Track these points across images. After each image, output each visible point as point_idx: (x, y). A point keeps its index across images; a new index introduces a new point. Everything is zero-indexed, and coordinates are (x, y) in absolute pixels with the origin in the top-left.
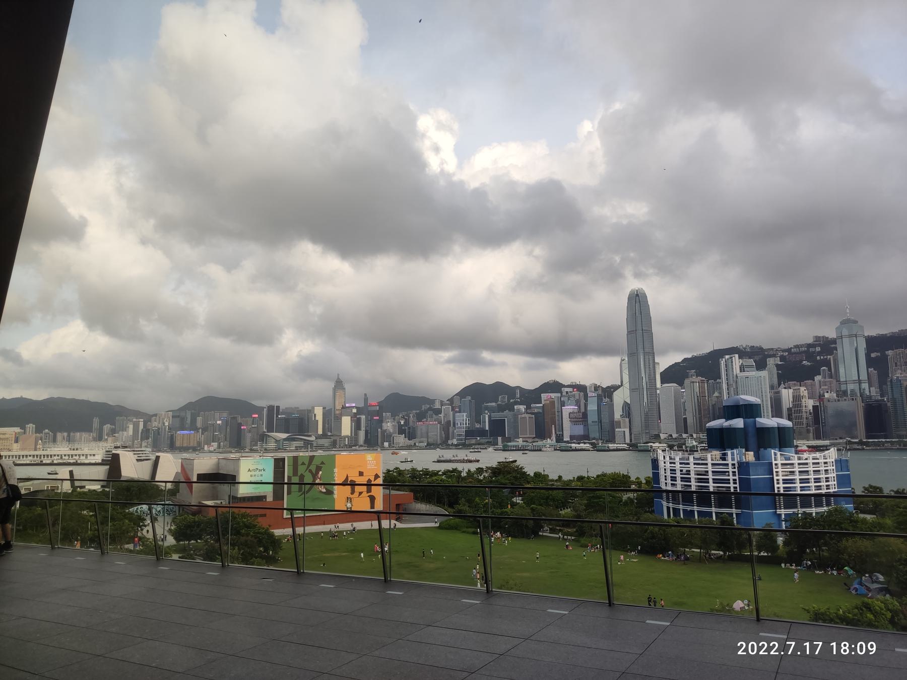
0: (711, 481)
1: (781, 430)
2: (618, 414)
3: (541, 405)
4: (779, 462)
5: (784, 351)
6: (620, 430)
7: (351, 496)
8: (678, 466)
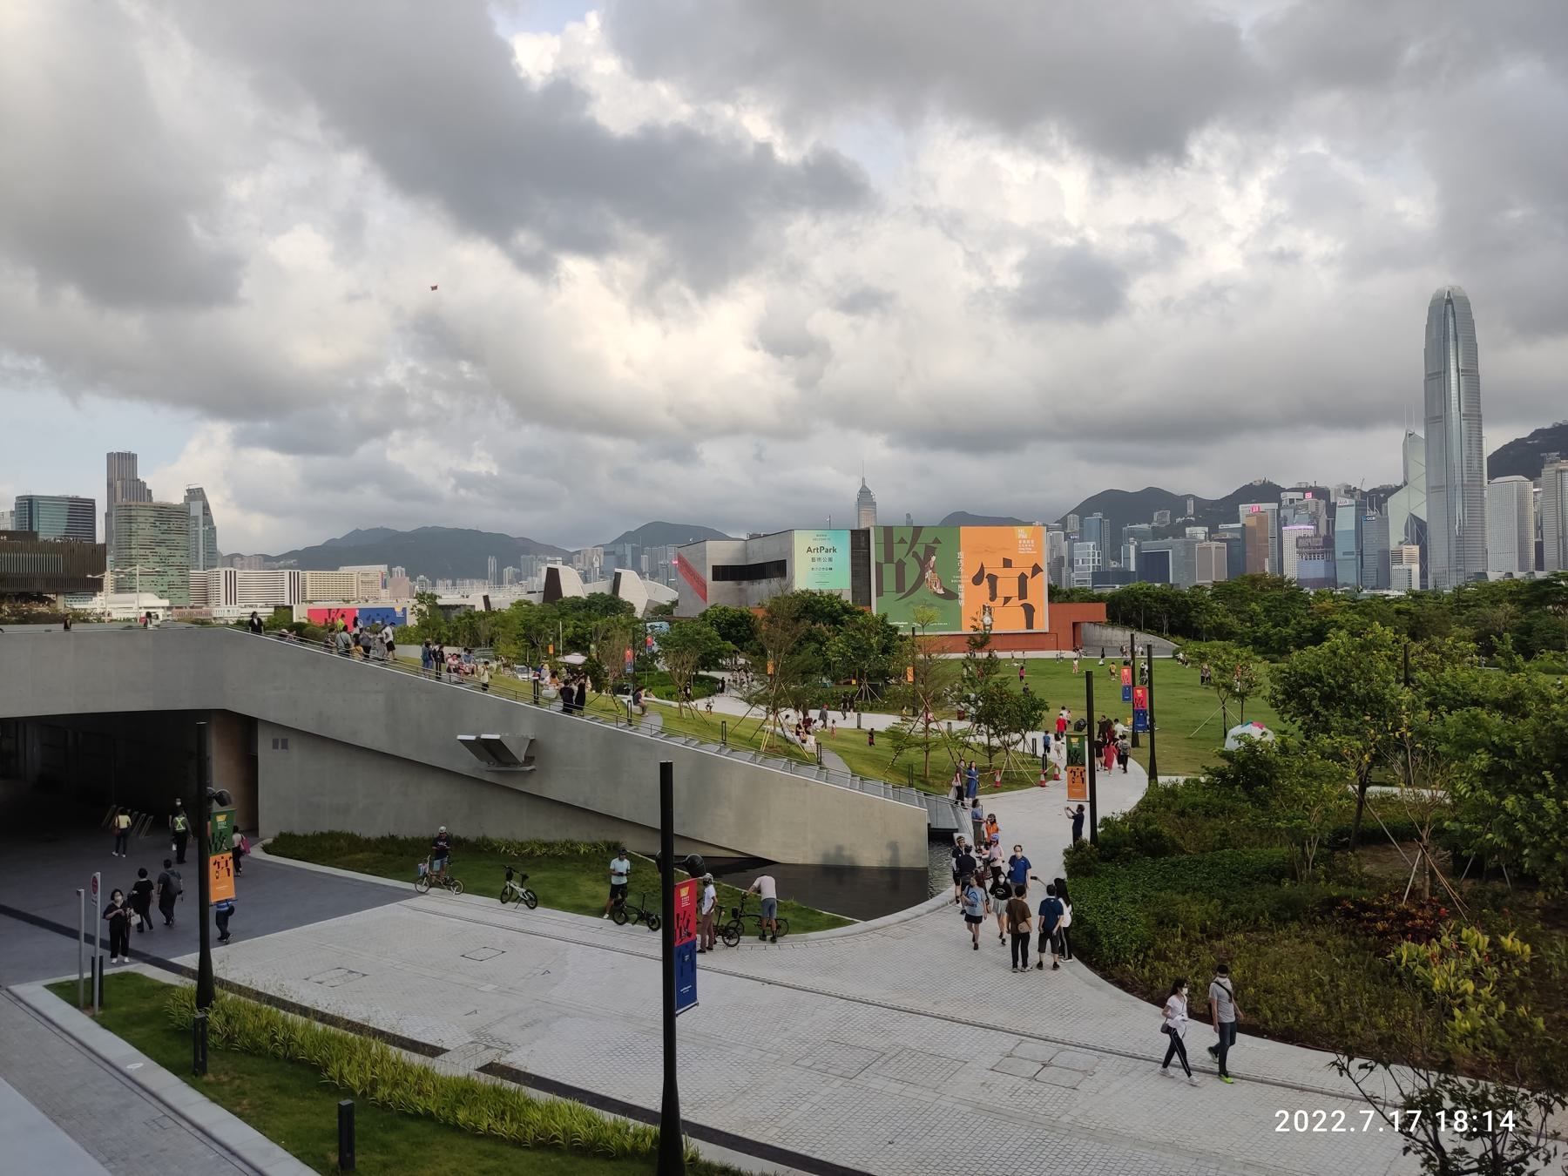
2: (1396, 535)
3: (1239, 525)
6: (1401, 567)
7: (991, 604)
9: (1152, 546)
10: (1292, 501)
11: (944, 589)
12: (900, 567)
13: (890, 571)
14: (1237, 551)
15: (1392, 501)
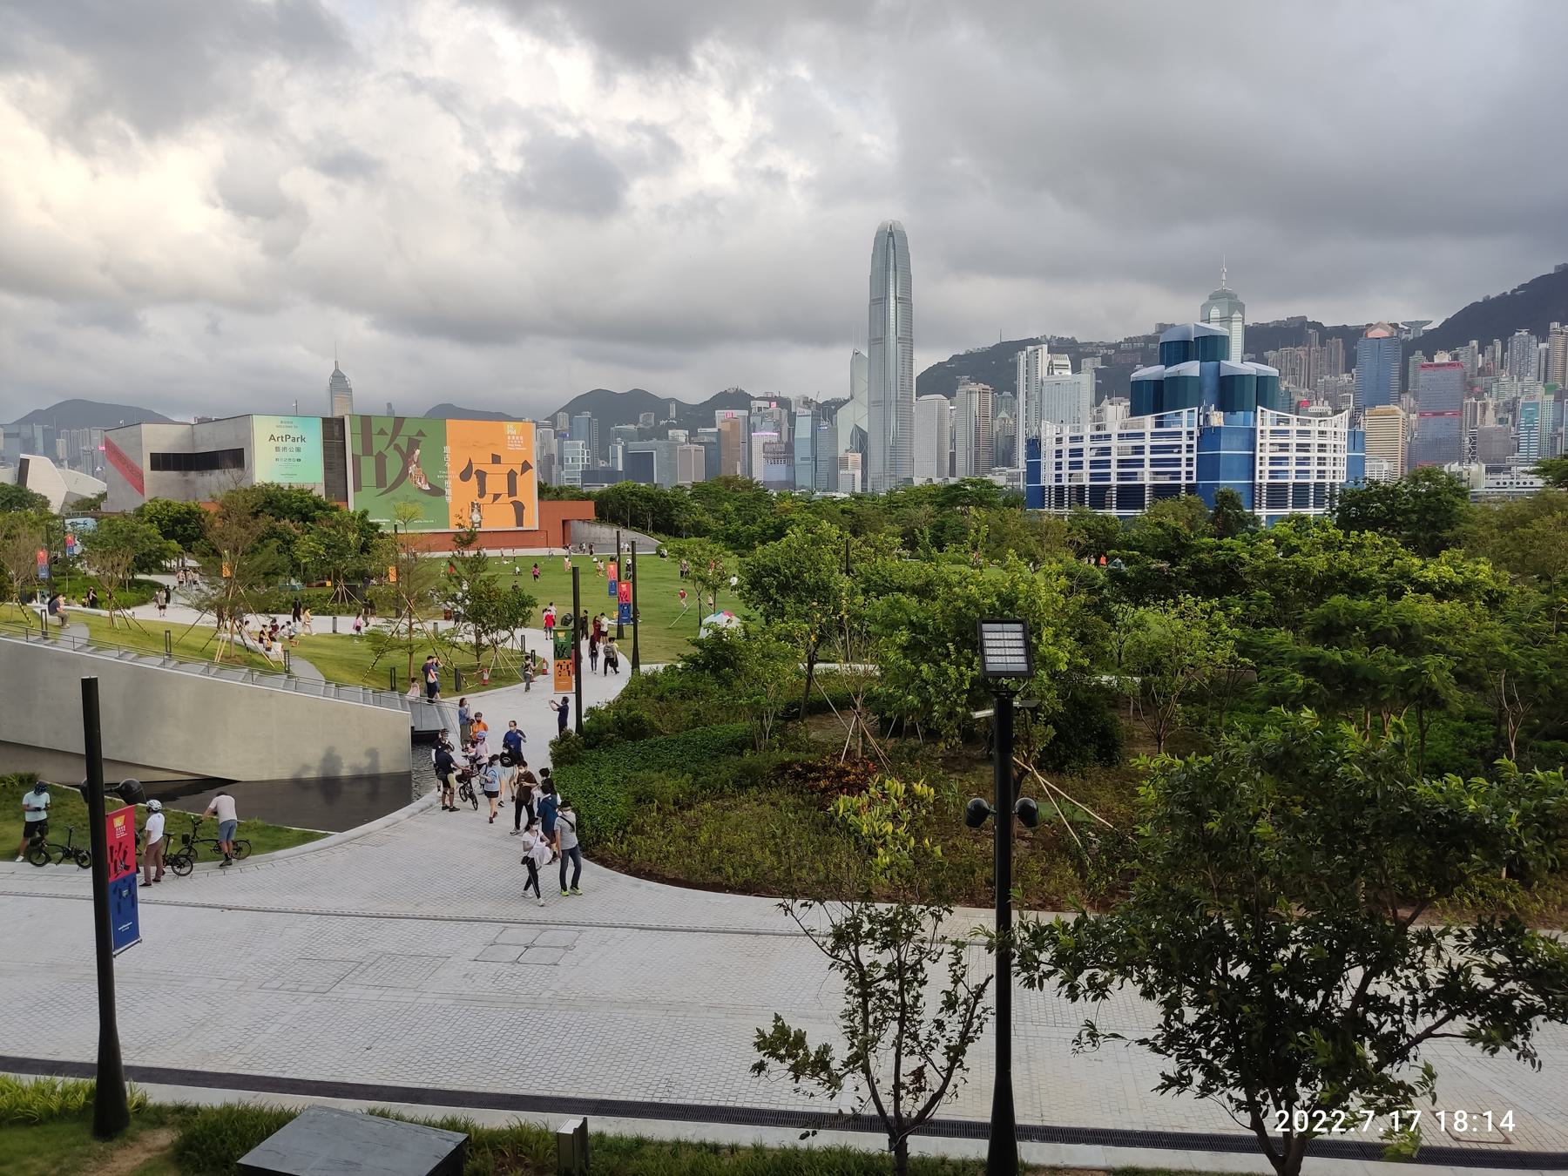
0: (1147, 463)
1: (1262, 381)
2: (844, 442)
3: (715, 430)
4: (1268, 427)
5: (1109, 347)
6: (846, 472)
8: (1086, 444)
9: (638, 446)
10: (760, 409)
11: (430, 485)
12: (381, 461)
13: (368, 465)
14: (714, 453)
15: (842, 414)
